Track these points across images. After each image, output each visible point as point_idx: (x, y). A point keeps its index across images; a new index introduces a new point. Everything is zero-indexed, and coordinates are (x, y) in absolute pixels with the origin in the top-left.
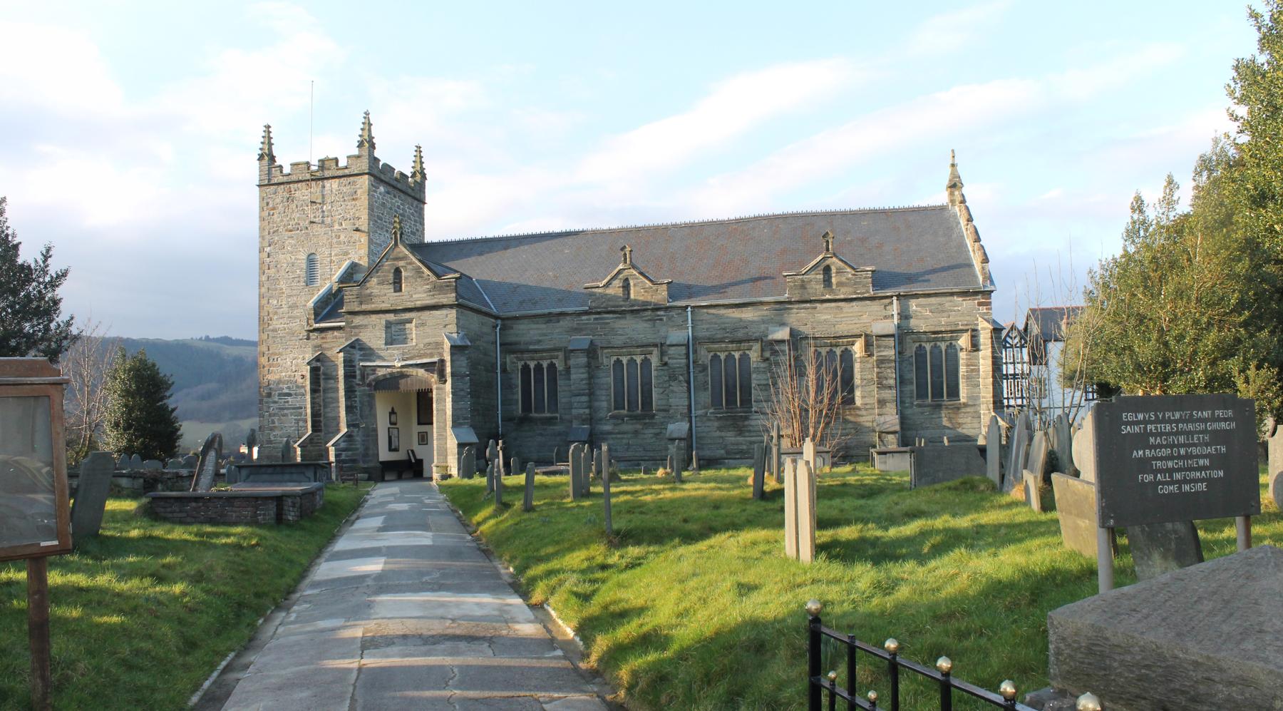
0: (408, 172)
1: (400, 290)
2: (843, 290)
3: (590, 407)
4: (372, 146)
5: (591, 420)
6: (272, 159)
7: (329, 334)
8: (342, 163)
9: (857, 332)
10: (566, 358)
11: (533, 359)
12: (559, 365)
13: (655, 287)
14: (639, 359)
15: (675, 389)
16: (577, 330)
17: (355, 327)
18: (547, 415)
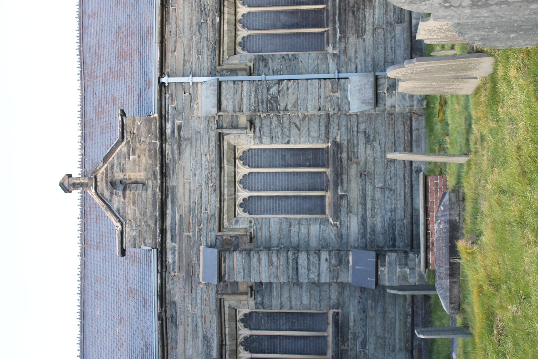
3: (318, 253)
5: (340, 251)
10: (234, 289)
12: (246, 306)
13: (128, 137)
14: (243, 170)
16: (190, 274)
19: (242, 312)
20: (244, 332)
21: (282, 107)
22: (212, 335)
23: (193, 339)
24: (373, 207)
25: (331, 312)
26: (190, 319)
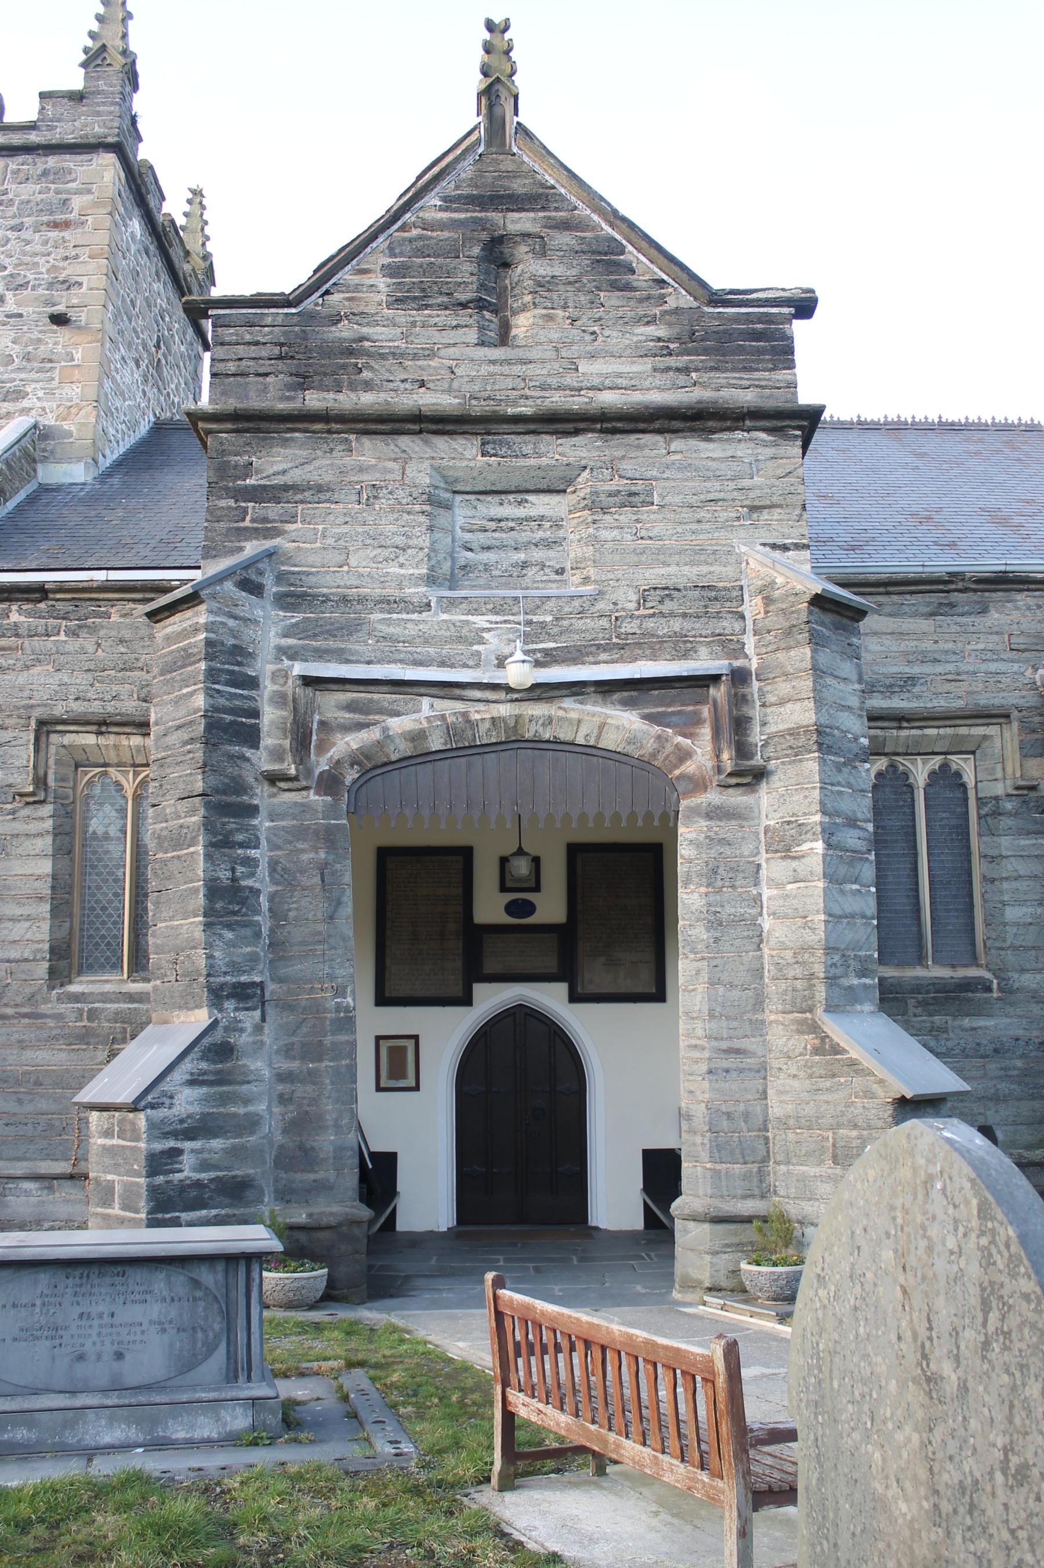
1: (504, 338)
4: (132, 78)
17: (257, 494)
19: (966, 767)
20: (920, 772)
22: (919, 697)
23: (906, 654)
26: (950, 646)
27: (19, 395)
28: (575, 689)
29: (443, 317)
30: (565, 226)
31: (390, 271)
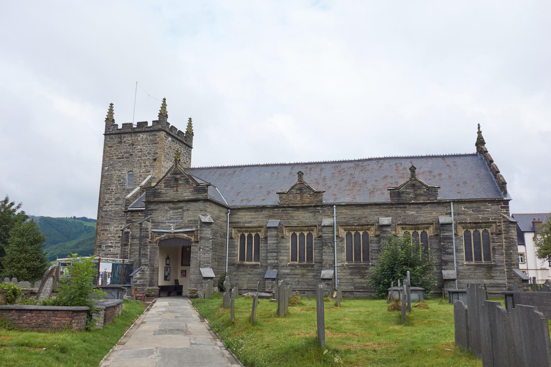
0: (184, 131)
1: (177, 191)
2: (422, 198)
3: (277, 259)
6: (113, 121)
7: (135, 215)
8: (150, 124)
9: (431, 221)
11: (247, 232)
14: (306, 234)
15: (326, 251)
16: (270, 217)
17: (150, 210)
18: (254, 263)
21: (324, 247)
24: (293, 278)
25: (259, 263)
27: (150, 172)
28: (180, 232)
29: (169, 189)
30: (183, 177)
31: (164, 183)
